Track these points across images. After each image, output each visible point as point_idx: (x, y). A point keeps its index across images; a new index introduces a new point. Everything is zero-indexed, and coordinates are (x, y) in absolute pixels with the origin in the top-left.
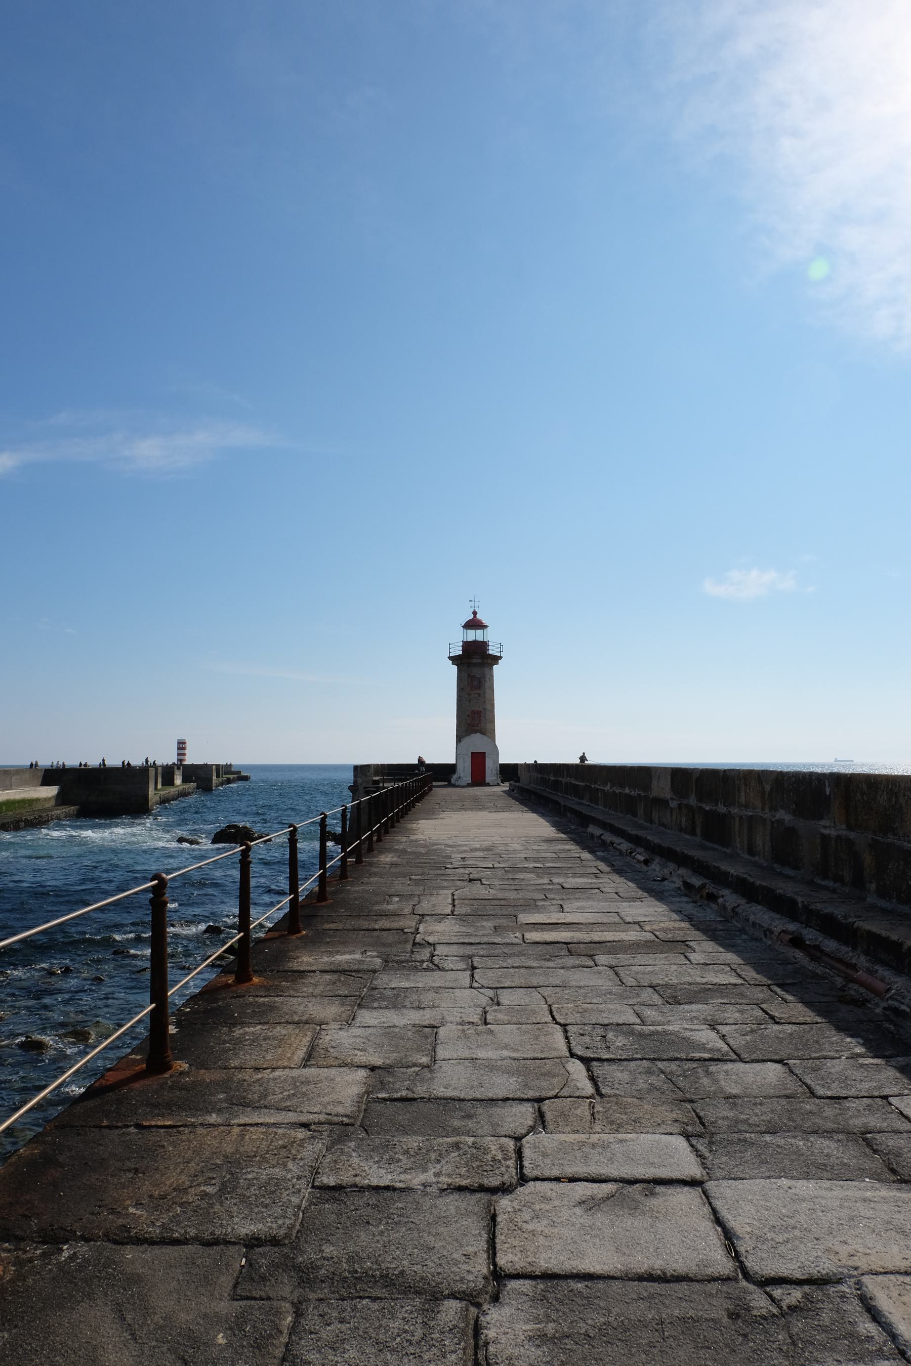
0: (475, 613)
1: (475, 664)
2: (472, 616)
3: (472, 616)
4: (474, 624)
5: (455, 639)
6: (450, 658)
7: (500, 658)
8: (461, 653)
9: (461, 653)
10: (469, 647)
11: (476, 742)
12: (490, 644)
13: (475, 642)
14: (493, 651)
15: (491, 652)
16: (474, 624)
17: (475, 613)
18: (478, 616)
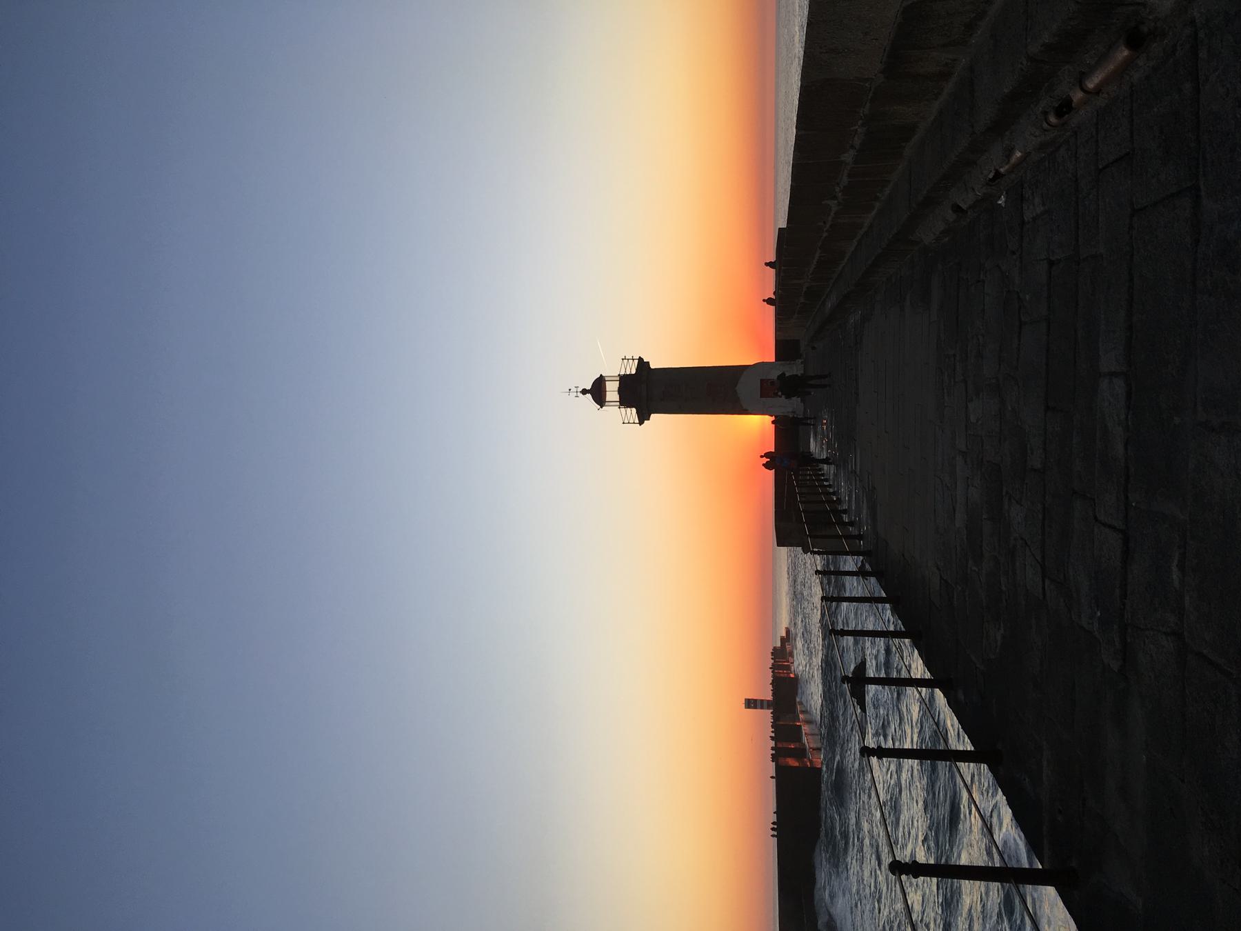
0: (584, 392)
1: (648, 391)
2: (589, 396)
3: (589, 396)
4: (597, 391)
5: (616, 416)
6: (641, 423)
7: (640, 359)
8: (634, 410)
9: (634, 410)
10: (625, 402)
11: (747, 388)
12: (622, 373)
13: (620, 391)
14: (632, 369)
15: (634, 372)
16: (597, 391)
17: (584, 392)
18: (589, 387)
